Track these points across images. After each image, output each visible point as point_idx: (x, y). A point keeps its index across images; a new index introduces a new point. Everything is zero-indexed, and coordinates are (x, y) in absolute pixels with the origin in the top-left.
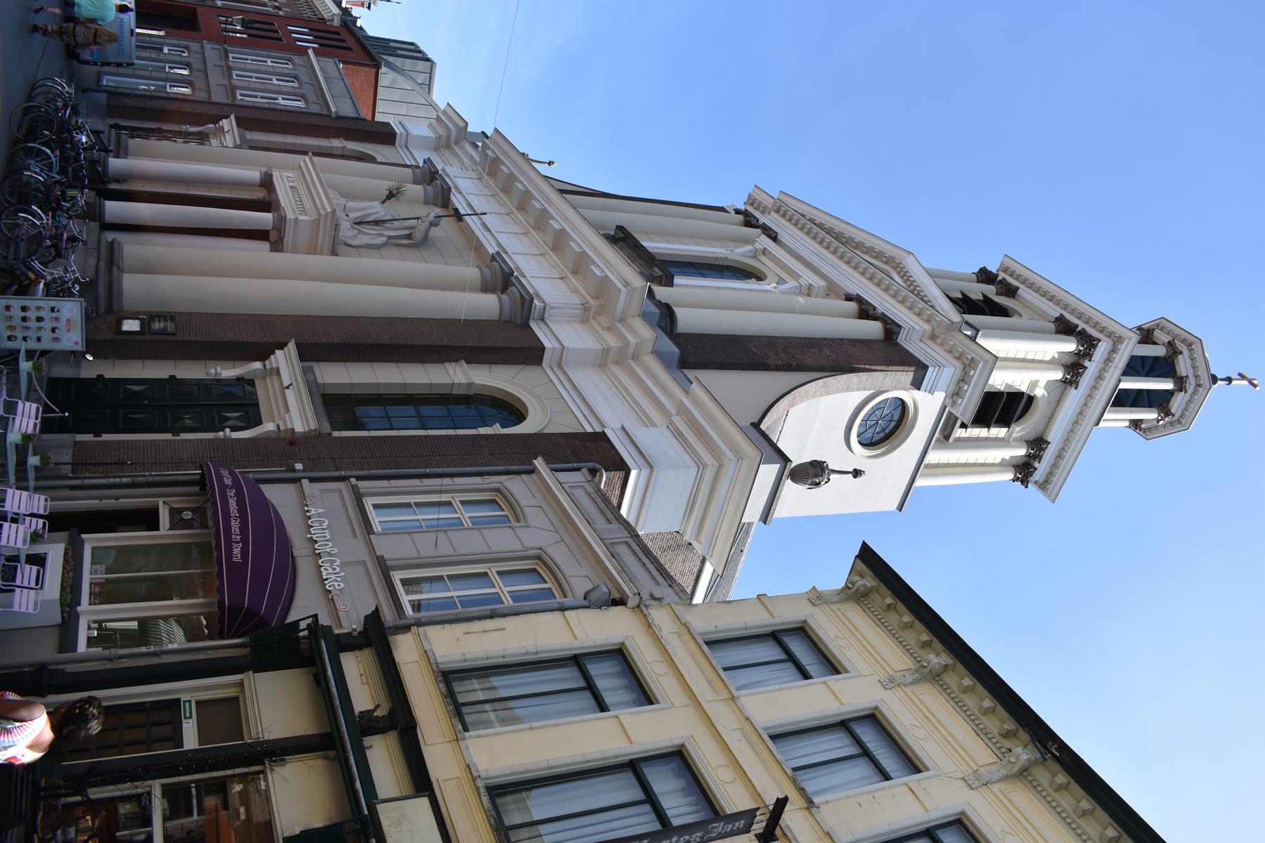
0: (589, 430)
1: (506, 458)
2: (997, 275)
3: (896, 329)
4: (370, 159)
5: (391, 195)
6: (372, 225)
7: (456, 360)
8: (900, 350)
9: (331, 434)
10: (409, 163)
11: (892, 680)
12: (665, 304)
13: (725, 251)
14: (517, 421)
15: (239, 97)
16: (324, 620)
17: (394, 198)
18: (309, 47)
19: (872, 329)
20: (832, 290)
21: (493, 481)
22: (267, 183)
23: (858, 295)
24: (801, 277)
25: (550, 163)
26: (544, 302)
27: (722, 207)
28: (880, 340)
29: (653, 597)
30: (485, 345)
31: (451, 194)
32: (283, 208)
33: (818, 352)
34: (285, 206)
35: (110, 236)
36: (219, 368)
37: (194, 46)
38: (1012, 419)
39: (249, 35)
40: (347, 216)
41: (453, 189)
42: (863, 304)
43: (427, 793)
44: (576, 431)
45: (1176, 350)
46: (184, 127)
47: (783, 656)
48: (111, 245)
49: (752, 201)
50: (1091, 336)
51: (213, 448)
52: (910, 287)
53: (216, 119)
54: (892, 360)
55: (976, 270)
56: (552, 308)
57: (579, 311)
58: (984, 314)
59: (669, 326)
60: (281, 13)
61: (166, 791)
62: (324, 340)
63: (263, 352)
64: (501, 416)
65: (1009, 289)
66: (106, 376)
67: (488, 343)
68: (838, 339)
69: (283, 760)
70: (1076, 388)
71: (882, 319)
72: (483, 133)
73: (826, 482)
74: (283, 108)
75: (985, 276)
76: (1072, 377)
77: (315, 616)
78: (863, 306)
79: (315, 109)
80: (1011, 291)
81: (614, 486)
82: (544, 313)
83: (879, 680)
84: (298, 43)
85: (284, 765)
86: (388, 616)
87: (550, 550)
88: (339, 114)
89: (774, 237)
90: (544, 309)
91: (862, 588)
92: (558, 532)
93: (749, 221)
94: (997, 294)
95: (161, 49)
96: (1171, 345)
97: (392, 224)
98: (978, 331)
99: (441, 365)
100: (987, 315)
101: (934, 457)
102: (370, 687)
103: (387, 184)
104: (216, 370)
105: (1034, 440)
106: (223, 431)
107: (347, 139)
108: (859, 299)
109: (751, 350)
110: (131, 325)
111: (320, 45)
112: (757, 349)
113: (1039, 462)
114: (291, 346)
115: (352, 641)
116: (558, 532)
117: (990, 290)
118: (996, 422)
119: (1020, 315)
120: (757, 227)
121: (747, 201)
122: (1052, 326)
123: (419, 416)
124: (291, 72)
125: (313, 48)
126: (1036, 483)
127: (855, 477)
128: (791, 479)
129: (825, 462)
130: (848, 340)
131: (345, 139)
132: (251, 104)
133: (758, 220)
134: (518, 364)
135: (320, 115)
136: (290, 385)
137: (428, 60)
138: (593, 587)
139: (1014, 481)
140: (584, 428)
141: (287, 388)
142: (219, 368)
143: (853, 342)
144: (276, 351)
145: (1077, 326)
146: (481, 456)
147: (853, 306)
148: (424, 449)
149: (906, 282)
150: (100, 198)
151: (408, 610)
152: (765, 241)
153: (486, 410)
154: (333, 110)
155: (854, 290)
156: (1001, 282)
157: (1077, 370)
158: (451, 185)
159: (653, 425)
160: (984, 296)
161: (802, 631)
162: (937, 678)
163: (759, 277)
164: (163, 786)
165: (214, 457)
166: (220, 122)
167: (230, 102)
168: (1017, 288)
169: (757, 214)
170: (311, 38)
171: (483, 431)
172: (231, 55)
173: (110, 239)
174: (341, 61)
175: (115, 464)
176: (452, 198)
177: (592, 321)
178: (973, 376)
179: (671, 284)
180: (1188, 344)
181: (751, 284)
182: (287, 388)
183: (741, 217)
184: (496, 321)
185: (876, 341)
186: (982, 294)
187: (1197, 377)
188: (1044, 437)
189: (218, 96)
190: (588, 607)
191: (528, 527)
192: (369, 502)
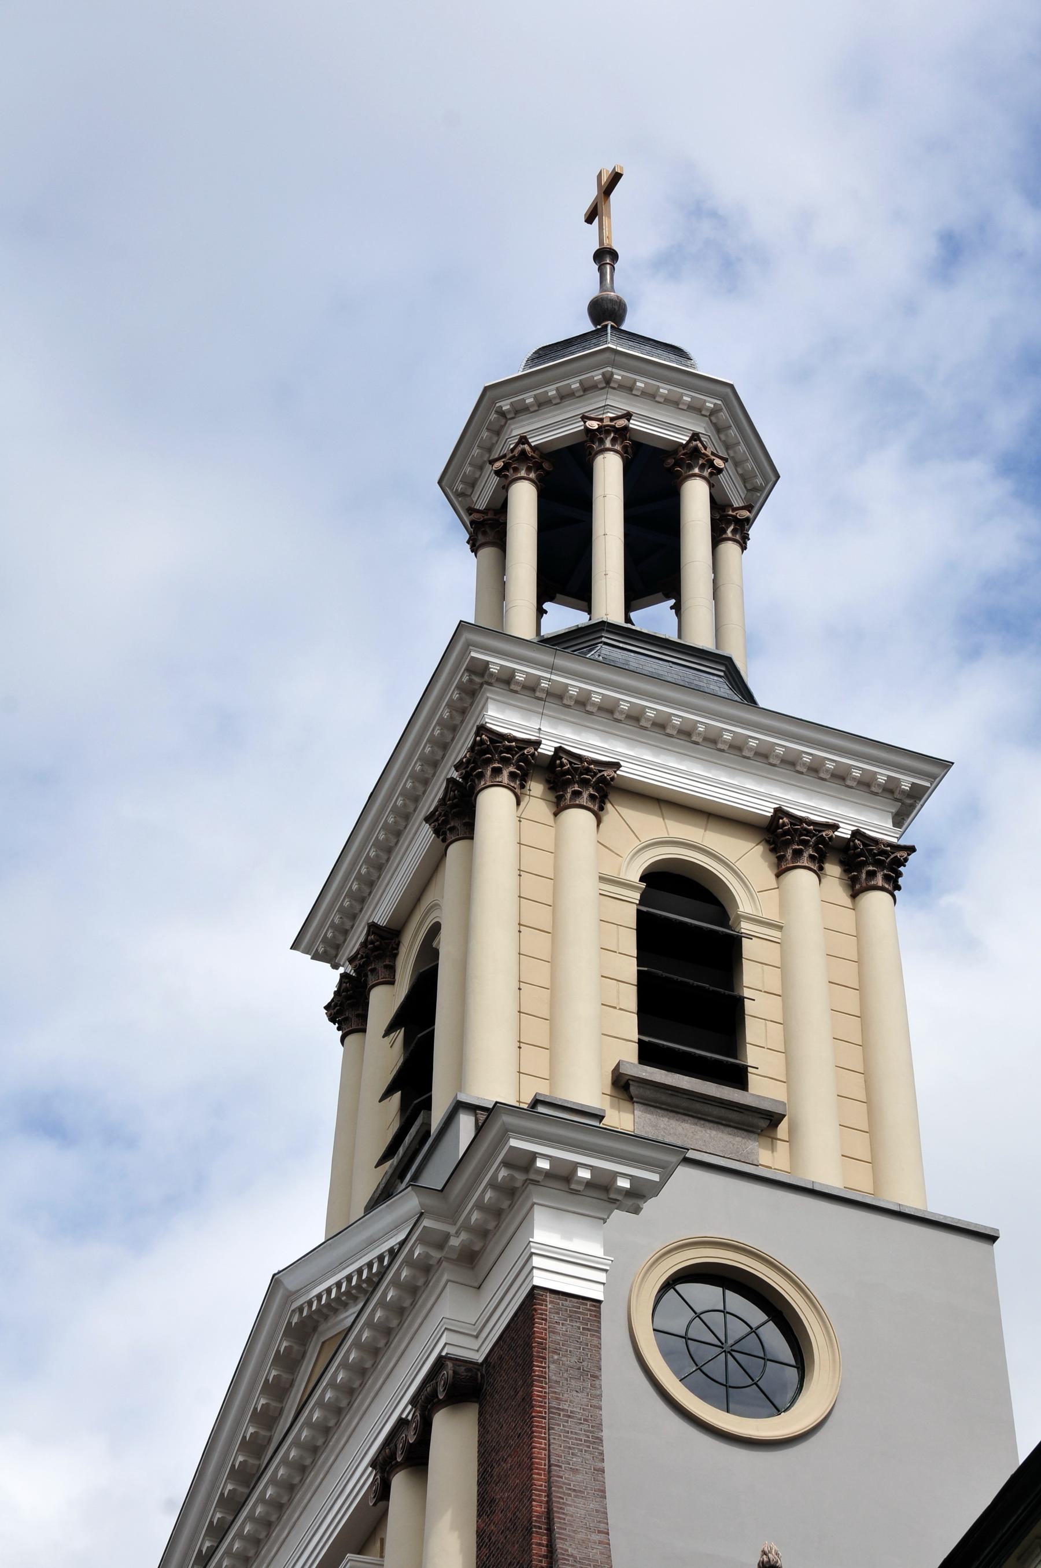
3: (448, 1371)
23: (373, 1464)
28: (480, 1414)
45: (516, 453)
50: (472, 749)
52: (365, 1291)
55: (333, 1032)
70: (617, 766)
76: (585, 783)
94: (392, 983)
96: (506, 467)
113: (835, 827)
122: (455, 850)
126: (900, 819)
130: (479, 1516)
145: (451, 781)
147: (399, 1482)
149: (355, 1299)
157: (568, 772)
168: (373, 927)
180: (503, 421)
187: (588, 389)
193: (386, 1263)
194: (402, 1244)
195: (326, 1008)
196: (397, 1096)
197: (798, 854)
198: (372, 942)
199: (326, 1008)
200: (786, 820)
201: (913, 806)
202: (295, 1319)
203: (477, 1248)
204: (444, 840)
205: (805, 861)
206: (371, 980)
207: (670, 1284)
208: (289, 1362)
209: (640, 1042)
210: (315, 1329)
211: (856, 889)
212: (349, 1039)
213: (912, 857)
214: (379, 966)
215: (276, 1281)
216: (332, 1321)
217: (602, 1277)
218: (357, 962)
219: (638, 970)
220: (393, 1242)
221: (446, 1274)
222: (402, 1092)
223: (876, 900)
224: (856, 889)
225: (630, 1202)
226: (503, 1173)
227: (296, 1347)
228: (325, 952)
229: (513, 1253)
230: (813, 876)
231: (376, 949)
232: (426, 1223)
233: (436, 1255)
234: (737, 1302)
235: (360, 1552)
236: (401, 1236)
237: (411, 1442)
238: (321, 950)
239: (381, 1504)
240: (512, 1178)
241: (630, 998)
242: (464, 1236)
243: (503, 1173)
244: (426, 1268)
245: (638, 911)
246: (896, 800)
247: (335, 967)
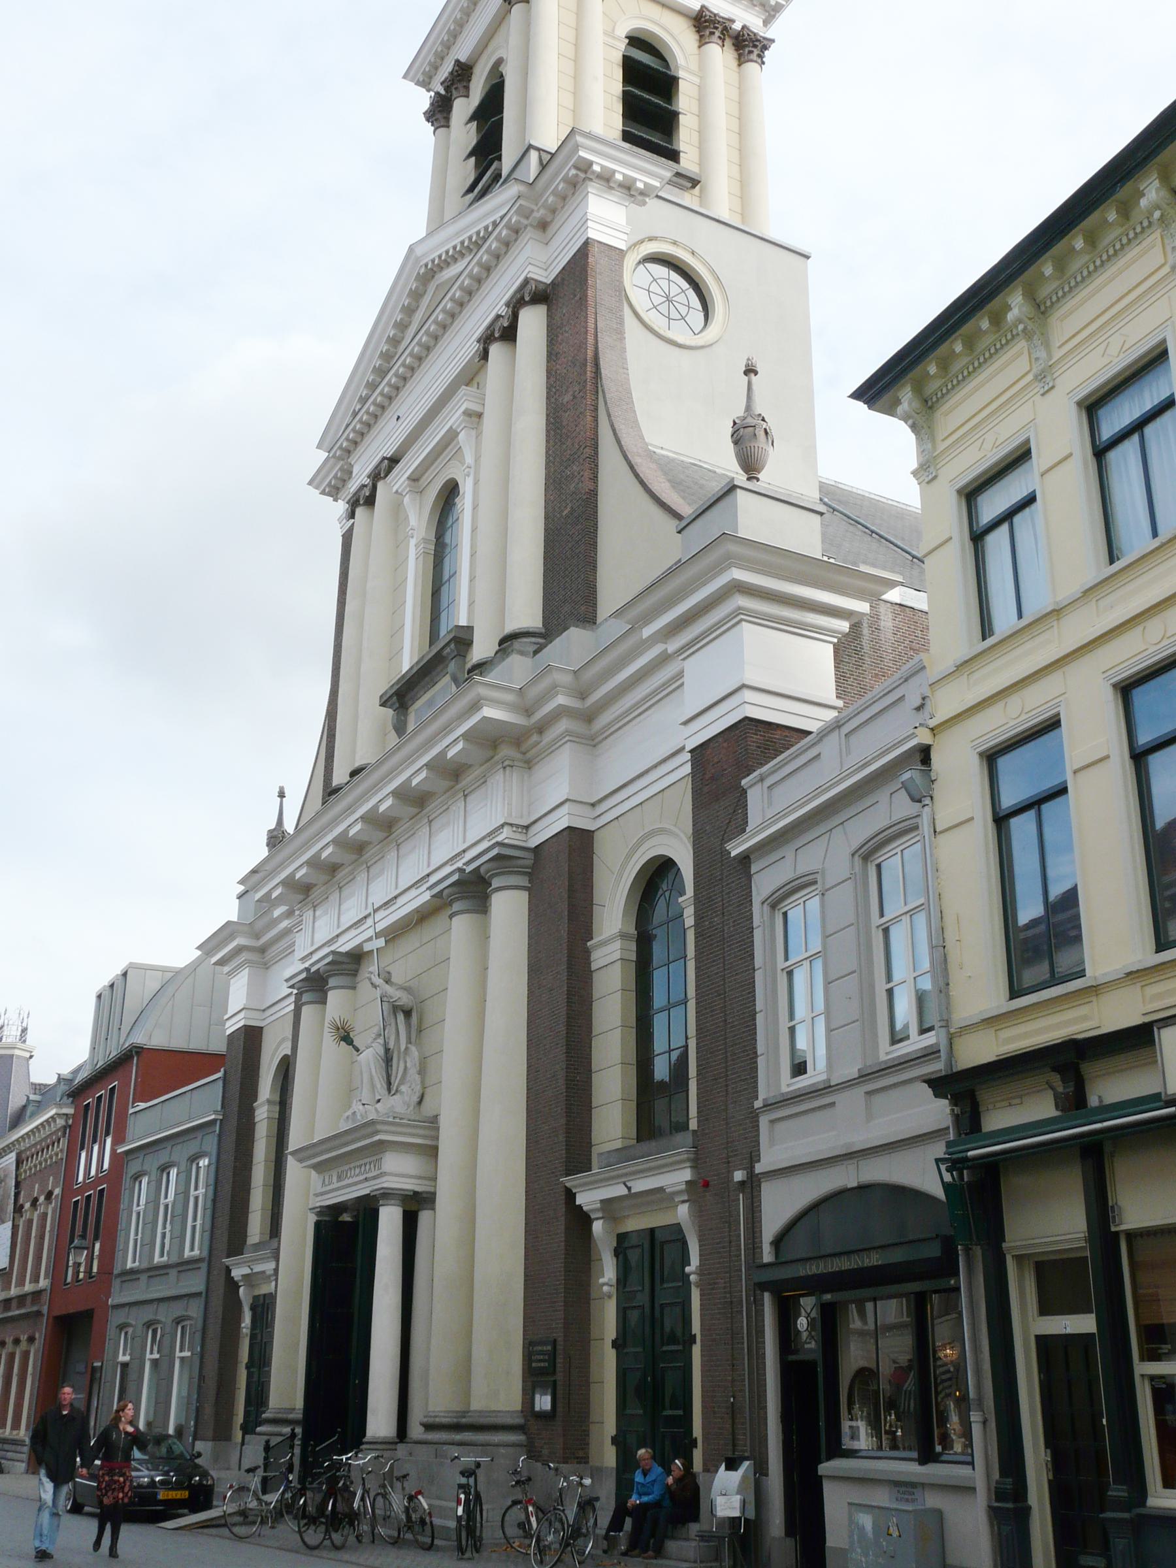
0: (688, 769)
1: (729, 893)
2: (437, 93)
4: (286, 1069)
5: (347, 1039)
6: (392, 1070)
7: (587, 953)
8: (563, 279)
9: (694, 1131)
10: (292, 1007)
11: (1041, 377)
12: (500, 643)
13: (413, 542)
14: (674, 871)
15: (196, 1252)
16: (939, 1149)
17: (351, 1035)
18: (113, 1151)
19: (532, 322)
20: (471, 375)
21: (759, 913)
24: (451, 427)
25: (282, 795)
26: (502, 826)
27: (343, 536)
28: (548, 310)
29: (919, 708)
30: (566, 913)
31: (340, 950)
32: (372, 1191)
33: (568, 413)
34: (371, 1189)
35: (416, 1431)
36: (601, 1281)
37: (116, 1318)
38: (666, 74)
39: (96, 1238)
40: (379, 1101)
41: (332, 948)
42: (492, 334)
43: (1155, 1030)
44: (690, 786)
46: (244, 1330)
47: (1005, 527)
48: (428, 1427)
49: (334, 491)
51: (713, 1289)
53: (232, 1286)
54: (578, 297)
55: (429, 128)
56: (510, 815)
57: (514, 775)
58: (499, 125)
59: (533, 640)
60: (57, 1191)
61: (1152, 1356)
62: (562, 1138)
63: (580, 1220)
64: (667, 894)
65: (459, 75)
66: (614, 1432)
67: (563, 907)
68: (548, 378)
69: (1112, 1207)
71: (514, 307)
72: (240, 897)
73: (763, 420)
74: (211, 1188)
75: (439, 112)
77: (937, 1161)
78: (497, 335)
79: (210, 1143)
80: (462, 74)
81: (767, 741)
82: (518, 826)
83: (1043, 395)
84: (106, 1166)
85: (1120, 1208)
86: (937, 1067)
87: (855, 845)
88: (219, 1108)
89: (393, 461)
90: (511, 825)
91: (913, 404)
92: (831, 830)
93: (366, 499)
94: (467, 96)
95: (125, 1366)
97: (389, 1038)
98: (530, 147)
99: (596, 977)
100: (501, 119)
101: (722, 201)
102: (1025, 1095)
103: (329, 1040)
104: (604, 1284)
105: (698, 32)
106: (688, 1275)
107: (255, 1097)
108: (487, 340)
109: (567, 516)
110: (543, 1402)
111: (107, 1134)
112: (566, 507)
113: (733, 21)
114: (570, 1181)
115: (967, 1115)
116: (831, 830)
117: (463, 108)
118: (670, 142)
119: (499, 62)
120: (374, 488)
121: (332, 496)
122: (517, 9)
123: (668, 1008)
124: (153, 1178)
125: (114, 1144)
126: (766, 23)
127: (756, 373)
128: (759, 473)
129: (735, 423)
130: (548, 362)
131: (256, 1100)
132: (207, 1235)
133: (364, 486)
134: (592, 864)
135: (220, 1136)
136: (626, 1186)
137: (125, 974)
138: (903, 789)
139: (763, 63)
140: (685, 776)
141: (629, 1189)
142: (601, 1281)
143: (552, 355)
144: (577, 1203)
146: (726, 928)
147: (495, 350)
148: (716, 1005)
150: (363, 1444)
151: (930, 1039)
152: (399, 478)
153: (660, 912)
154: (213, 1117)
155: (471, 347)
156: (447, 89)
158: (326, 950)
159: (680, 674)
160: (472, 119)
161: (971, 494)
162: (1043, 308)
163: (451, 492)
164: (1142, 1359)
165: (725, 1288)
166: (235, 1279)
167: (204, 1266)
168: (458, 62)
169: (353, 487)
170: (96, 1148)
171: (689, 920)
172: (129, 1265)
173: (422, 1429)
174: (133, 1103)
175: (733, 1418)
176: (344, 949)
177: (529, 755)
178: (602, 167)
179: (470, 629)
181: (465, 503)
182: (629, 1189)
183: (359, 511)
184: (529, 895)
185: (550, 316)
186: (467, 123)
188: (694, 15)
189: (195, 1282)
190: (932, 797)
191: (823, 870)
192: (789, 1084)
193: (490, 229)
194: (502, 218)
195: (424, 114)
196: (473, 159)
197: (712, 33)
198: (457, 71)
199: (424, 114)
200: (707, 13)
201: (774, 16)
202: (423, 270)
203: (549, 220)
204: (509, 4)
205: (715, 38)
206: (455, 93)
207: (639, 263)
208: (417, 295)
209: (624, 131)
210: (433, 277)
211: (741, 61)
212: (439, 130)
213: (773, 46)
214: (459, 85)
215: (411, 249)
216: (444, 273)
217: (625, 237)
218: (446, 84)
219: (623, 91)
220: (496, 216)
221: (529, 234)
222: (476, 159)
223: (752, 67)
224: (741, 61)
225: (640, 198)
226: (573, 172)
227: (421, 287)
228: (424, 80)
229: (574, 220)
230: (720, 49)
231: (459, 75)
232: (520, 202)
233: (525, 222)
234: (674, 276)
235: (466, 386)
236: (505, 211)
237: (505, 325)
238: (421, 79)
239: (482, 361)
240: (577, 175)
241: (619, 108)
242: (542, 211)
243: (573, 172)
244: (517, 231)
245: (624, 56)
246: (766, 11)
247: (428, 90)
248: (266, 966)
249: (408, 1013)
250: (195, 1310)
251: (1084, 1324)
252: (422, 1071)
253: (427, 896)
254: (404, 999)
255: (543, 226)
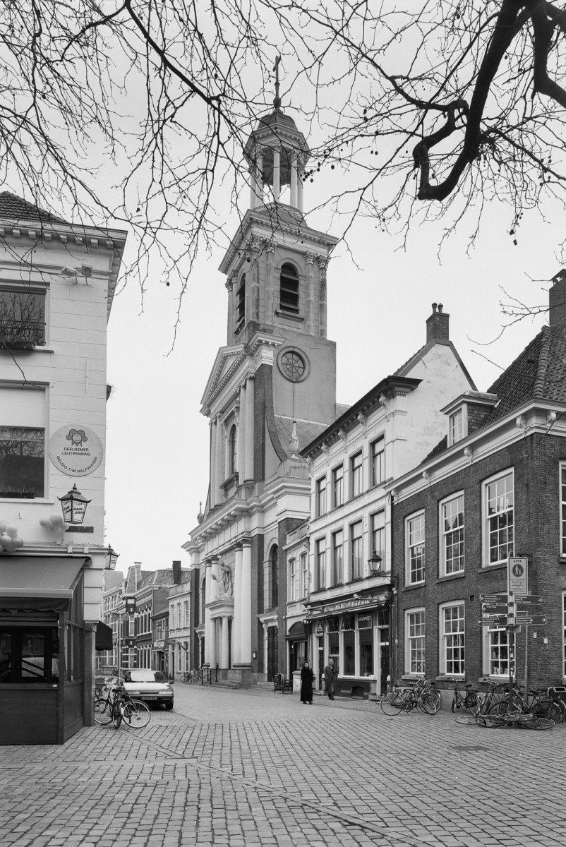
7: (262, 564)
21: (288, 563)
22: (215, 619)
35: (232, 668)
48: (234, 666)
53: (196, 634)
181: (238, 428)
248: (199, 552)
249: (228, 573)
250: (188, 640)
251: (387, 644)
252: (232, 587)
253: (230, 546)
254: (227, 570)
255: (252, 355)
